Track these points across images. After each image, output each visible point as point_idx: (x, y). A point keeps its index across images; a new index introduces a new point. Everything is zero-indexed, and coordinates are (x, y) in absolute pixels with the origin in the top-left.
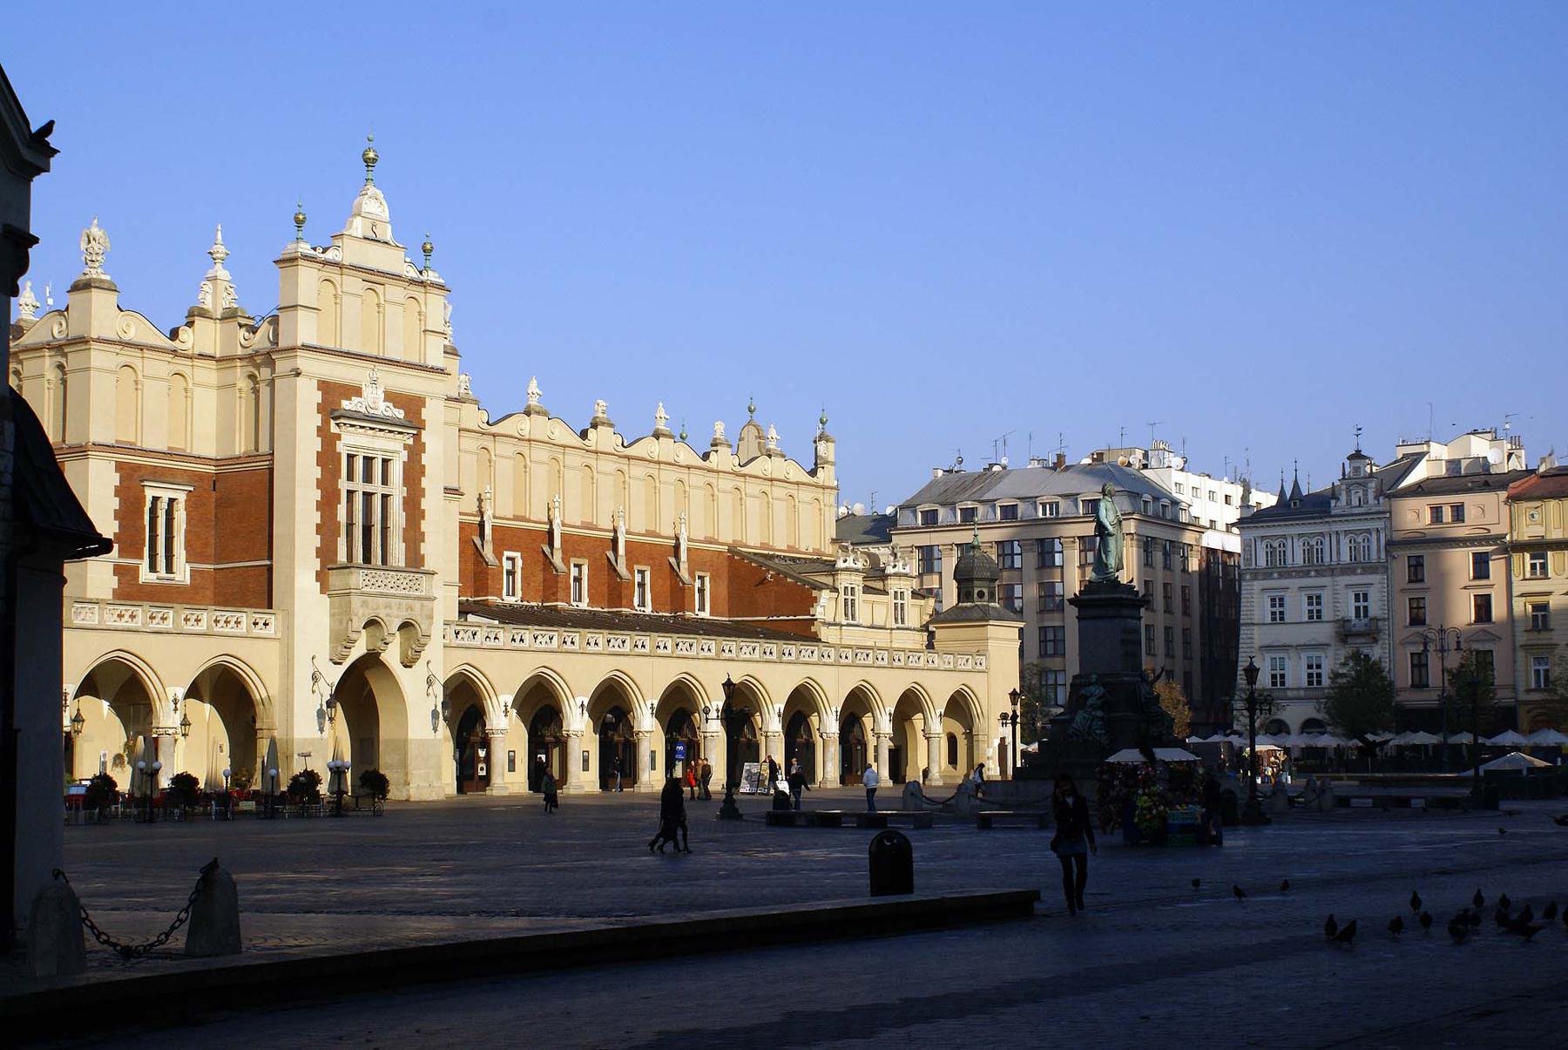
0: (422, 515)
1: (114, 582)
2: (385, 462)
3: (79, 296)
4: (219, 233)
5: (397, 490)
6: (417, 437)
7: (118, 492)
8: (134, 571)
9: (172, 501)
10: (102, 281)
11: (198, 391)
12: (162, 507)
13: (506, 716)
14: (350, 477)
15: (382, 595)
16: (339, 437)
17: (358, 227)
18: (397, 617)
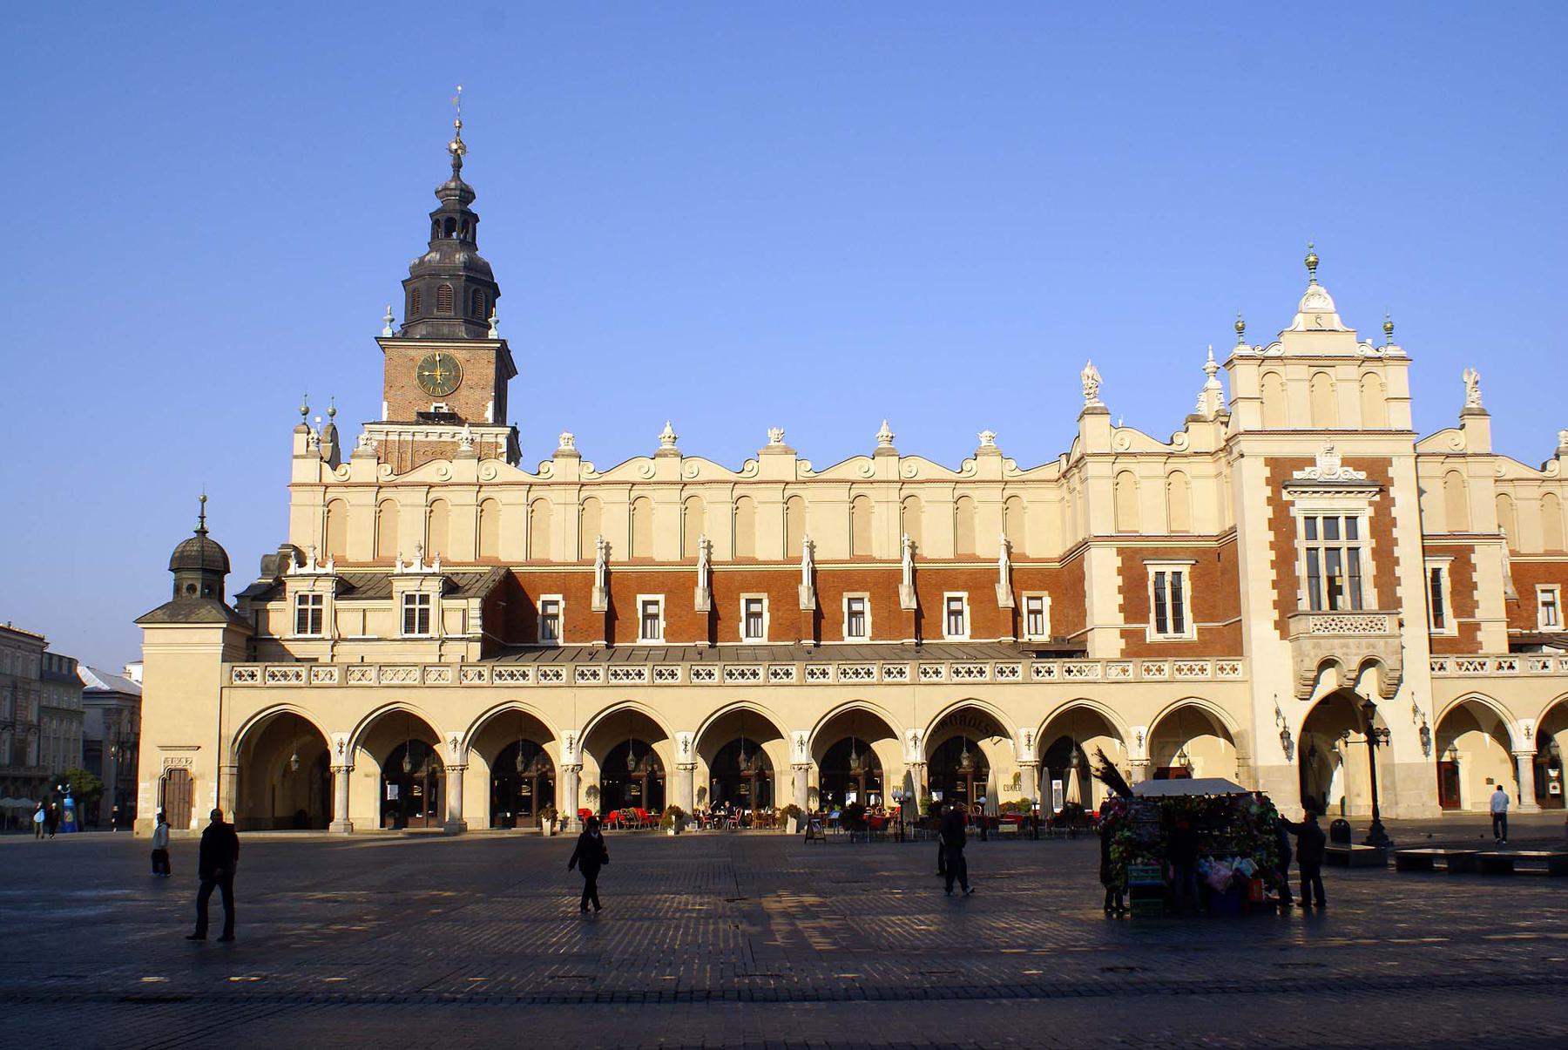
0: (1396, 562)
1: (1122, 644)
2: (1351, 520)
3: (1082, 422)
4: (1210, 352)
5: (1366, 542)
6: (1383, 491)
7: (1120, 572)
8: (1143, 632)
9: (1177, 575)
10: (1095, 408)
11: (1195, 484)
12: (1168, 578)
13: (1528, 738)
14: (1311, 534)
15: (1335, 637)
16: (1292, 503)
17: (1300, 322)
18: (1356, 655)
